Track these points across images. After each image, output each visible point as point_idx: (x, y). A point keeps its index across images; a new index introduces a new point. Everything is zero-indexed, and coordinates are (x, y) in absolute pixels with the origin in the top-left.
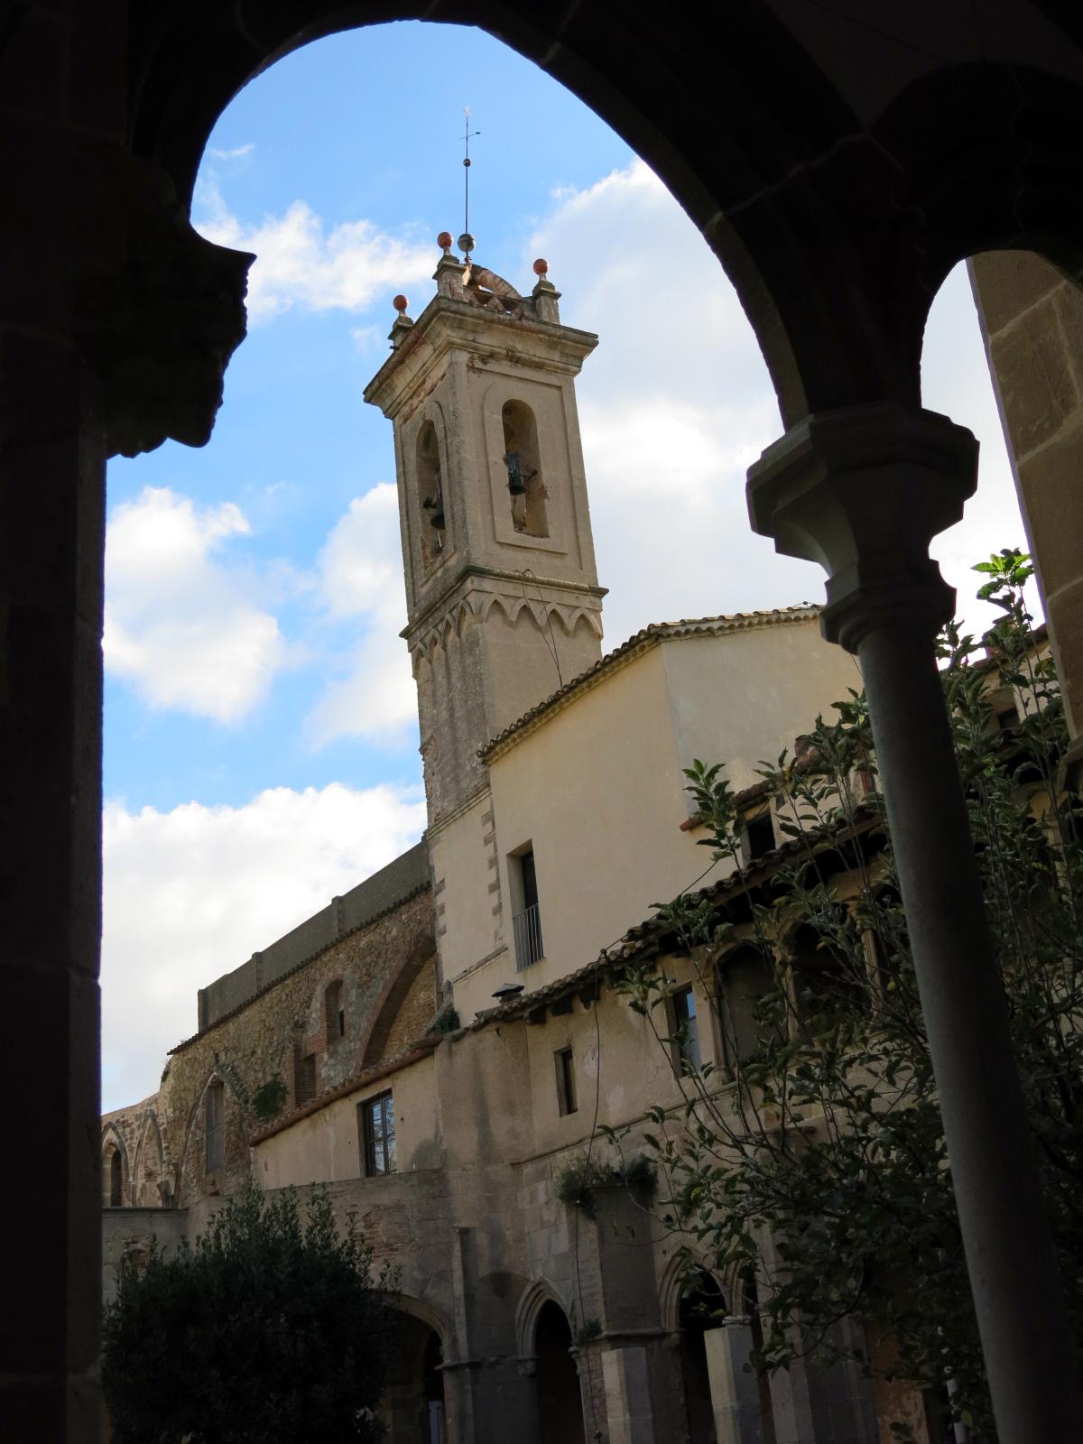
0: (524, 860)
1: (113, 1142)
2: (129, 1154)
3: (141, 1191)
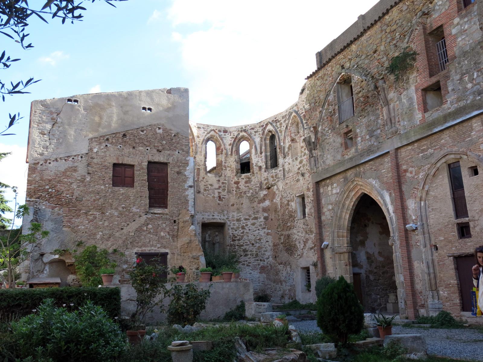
1: (271, 130)
2: (280, 134)
3: (289, 148)
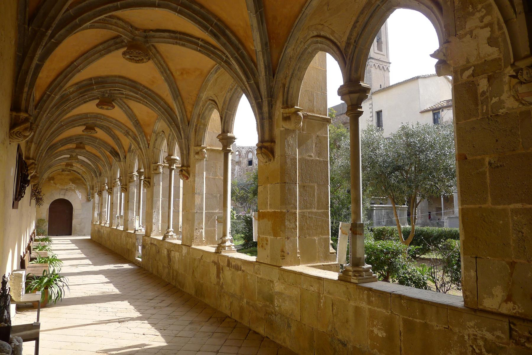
0: (379, 114)
